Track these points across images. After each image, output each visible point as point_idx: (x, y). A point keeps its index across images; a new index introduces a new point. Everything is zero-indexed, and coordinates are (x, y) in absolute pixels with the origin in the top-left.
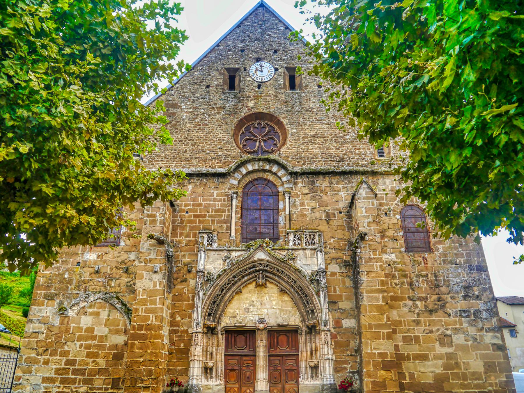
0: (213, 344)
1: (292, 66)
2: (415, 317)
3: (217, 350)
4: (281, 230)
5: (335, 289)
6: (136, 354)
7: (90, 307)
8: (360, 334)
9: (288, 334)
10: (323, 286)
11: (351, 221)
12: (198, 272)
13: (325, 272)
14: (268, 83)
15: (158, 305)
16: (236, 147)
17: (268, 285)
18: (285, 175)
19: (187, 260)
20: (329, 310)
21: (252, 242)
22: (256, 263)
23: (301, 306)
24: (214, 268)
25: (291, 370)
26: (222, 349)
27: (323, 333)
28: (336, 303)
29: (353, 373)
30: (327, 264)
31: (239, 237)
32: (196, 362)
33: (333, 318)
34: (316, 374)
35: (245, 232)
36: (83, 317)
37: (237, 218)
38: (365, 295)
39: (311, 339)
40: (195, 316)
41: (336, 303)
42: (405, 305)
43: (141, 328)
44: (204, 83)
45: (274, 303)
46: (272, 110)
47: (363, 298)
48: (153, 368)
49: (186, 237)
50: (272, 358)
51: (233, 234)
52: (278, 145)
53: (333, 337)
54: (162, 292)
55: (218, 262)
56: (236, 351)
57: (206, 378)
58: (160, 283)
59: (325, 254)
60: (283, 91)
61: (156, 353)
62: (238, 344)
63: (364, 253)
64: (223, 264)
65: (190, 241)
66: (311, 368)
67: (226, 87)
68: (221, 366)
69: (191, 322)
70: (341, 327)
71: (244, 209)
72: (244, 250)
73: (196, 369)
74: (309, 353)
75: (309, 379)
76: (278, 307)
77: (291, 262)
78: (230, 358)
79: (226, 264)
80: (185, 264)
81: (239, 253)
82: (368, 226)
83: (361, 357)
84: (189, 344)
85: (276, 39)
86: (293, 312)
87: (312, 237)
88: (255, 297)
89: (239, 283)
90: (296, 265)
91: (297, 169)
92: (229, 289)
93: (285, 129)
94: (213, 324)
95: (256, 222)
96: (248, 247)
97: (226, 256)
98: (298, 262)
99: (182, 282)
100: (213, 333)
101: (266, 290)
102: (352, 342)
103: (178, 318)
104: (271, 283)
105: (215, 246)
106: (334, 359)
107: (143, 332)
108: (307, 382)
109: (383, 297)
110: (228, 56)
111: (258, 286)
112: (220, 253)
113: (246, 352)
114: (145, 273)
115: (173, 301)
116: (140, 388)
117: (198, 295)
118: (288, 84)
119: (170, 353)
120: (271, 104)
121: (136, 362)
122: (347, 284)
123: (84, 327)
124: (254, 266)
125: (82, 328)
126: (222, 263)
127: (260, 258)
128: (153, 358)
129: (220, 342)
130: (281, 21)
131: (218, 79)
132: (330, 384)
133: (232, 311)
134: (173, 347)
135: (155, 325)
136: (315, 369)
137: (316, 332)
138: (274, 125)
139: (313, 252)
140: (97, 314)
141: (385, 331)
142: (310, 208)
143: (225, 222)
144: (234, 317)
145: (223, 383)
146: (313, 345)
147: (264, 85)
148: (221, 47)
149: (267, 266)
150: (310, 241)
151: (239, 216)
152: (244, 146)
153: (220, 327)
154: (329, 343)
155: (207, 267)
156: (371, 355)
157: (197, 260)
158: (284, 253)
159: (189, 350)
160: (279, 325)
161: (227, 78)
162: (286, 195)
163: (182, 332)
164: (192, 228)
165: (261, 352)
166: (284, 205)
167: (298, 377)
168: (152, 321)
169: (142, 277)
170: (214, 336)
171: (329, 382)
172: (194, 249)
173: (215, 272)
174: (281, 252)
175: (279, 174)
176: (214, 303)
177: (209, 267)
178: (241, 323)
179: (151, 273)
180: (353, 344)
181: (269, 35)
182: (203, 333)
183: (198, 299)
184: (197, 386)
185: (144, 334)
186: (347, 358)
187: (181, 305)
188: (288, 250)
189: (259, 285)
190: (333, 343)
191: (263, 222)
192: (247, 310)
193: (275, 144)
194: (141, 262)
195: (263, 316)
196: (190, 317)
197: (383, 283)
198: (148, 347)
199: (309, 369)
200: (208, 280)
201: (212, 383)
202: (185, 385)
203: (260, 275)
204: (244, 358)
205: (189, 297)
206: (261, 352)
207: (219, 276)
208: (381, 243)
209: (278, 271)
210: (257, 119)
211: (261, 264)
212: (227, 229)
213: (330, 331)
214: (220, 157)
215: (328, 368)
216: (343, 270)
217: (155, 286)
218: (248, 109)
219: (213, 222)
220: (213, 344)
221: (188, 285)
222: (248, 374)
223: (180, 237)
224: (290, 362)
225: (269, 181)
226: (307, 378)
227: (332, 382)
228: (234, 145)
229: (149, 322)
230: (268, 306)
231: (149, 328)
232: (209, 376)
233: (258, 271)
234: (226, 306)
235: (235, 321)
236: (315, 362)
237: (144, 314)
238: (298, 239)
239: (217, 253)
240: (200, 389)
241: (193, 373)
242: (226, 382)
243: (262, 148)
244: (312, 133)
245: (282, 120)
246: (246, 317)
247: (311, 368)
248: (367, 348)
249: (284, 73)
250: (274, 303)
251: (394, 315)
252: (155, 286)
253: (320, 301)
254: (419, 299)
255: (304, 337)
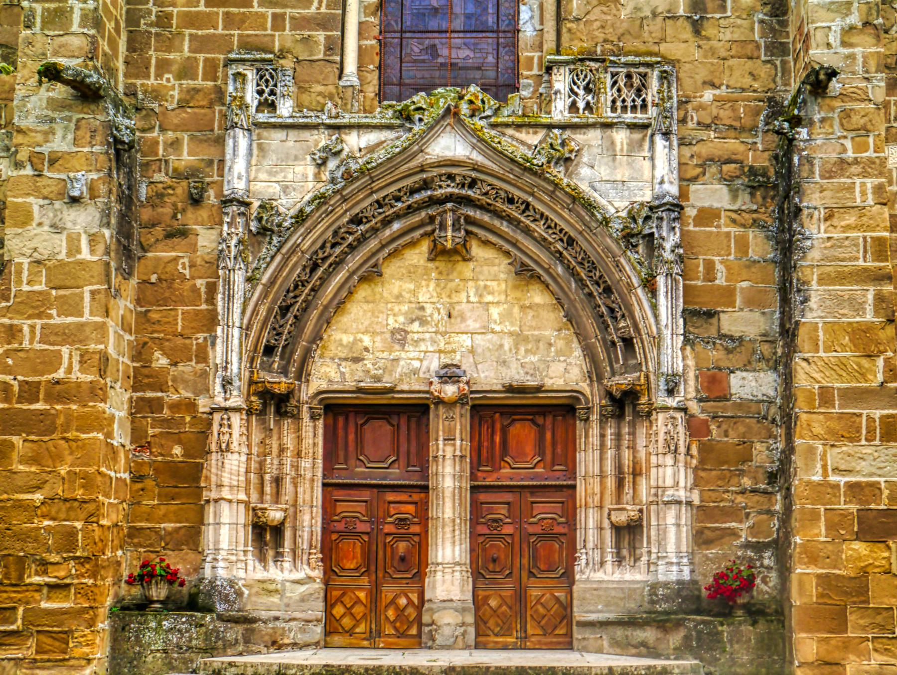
0: (282, 450)
3: (296, 468)
4: (524, 54)
5: (710, 267)
6: (19, 481)
8: (788, 420)
9: (540, 421)
10: (668, 255)
11: (784, 24)
12: (227, 202)
13: (677, 207)
15: (87, 317)
17: (476, 250)
19: (186, 158)
20: (687, 341)
21: (420, 99)
22: (435, 172)
23: (590, 325)
24: (285, 189)
25: (548, 536)
26: (312, 467)
27: (661, 418)
28: (710, 315)
29: (759, 548)
30: (685, 181)
31: (373, 78)
32: (225, 506)
33: (698, 368)
34: (633, 548)
35: (393, 61)
38: (816, 292)
39: (618, 436)
40: (217, 354)
41: (710, 315)
43: (30, 392)
45: (495, 312)
47: (806, 300)
48: (79, 525)
49: (180, 76)
50: (483, 497)
51: (351, 66)
53: (695, 428)
54: (99, 270)
55: (299, 169)
56: (361, 472)
57: (262, 558)
58: (93, 240)
59: (682, 143)
61: (85, 476)
62: (369, 449)
63: (822, 142)
64: (317, 177)
65: (197, 91)
66: (617, 529)
68: (310, 522)
69: (204, 374)
70: (725, 397)
72: (389, 127)
73: (225, 531)
74: (611, 483)
75: (609, 566)
76: (508, 327)
77: (557, 172)
78: (339, 494)
79: (326, 176)
80: (178, 175)
81: (373, 137)
82: (844, 44)
83: (788, 496)
84: (199, 445)
86: (561, 344)
87: (636, 81)
88: (427, 293)
89: (373, 244)
90: (574, 181)
92: (339, 263)
94: (281, 383)
95: (433, 24)
96: (405, 117)
97: (325, 149)
98: (585, 171)
99: (169, 236)
100: (281, 414)
101: (467, 269)
102: (758, 446)
103: (161, 361)
104: (486, 243)
105: (285, 108)
106: (697, 502)
107: (39, 406)
108: (599, 575)
109: (880, 298)
111: (438, 253)
112: (305, 134)
113: (395, 475)
114: (35, 203)
115: (139, 302)
116: (39, 588)
117: (228, 282)
119: (137, 478)
121: (20, 505)
122: (754, 253)
124: (426, 185)
126: (311, 170)
127: (449, 154)
128: (79, 493)
129: (308, 441)
132: (679, 582)
133: (346, 339)
134: (146, 457)
135: (79, 385)
136: (629, 535)
137: (637, 414)
139: (637, 136)
141: (877, 414)
143: (323, 23)
144: (357, 360)
145: (318, 574)
146: (626, 454)
149: (473, 184)
150: (629, 95)
153: (306, 392)
154: (682, 449)
155: (257, 187)
156: (825, 490)
157: (222, 161)
158: (534, 138)
159: (199, 468)
160: (510, 389)
163: (175, 407)
164: (200, 44)
165: (449, 476)
167: (572, 559)
168: (69, 370)
169: (25, 218)
170: (287, 423)
171: (673, 577)
172: (213, 120)
173: (288, 205)
174: (522, 135)
176: (285, 310)
177: (265, 187)
178: (378, 379)
179: (58, 205)
180: (763, 454)
182: (249, 412)
183: (230, 298)
184: (232, 583)
185: (42, 413)
186: (739, 498)
187: (167, 316)
188: (550, 127)
189: (445, 252)
190: (694, 451)
191: (458, 24)
192: (400, 337)
194: (18, 165)
195: (457, 358)
196: (202, 356)
197: (880, 248)
198: (57, 458)
199: (608, 534)
200: (264, 231)
201: (282, 573)
202: (192, 579)
204: (390, 497)
205: (195, 290)
206: (449, 476)
207: (301, 218)
208: (886, 105)
209: (511, 201)
211: (451, 177)
212: (329, 49)
213: (685, 410)
215: (672, 531)
216: (744, 201)
217: (74, 249)
219: (278, 19)
220: (282, 450)
221: (194, 248)
222: (402, 547)
223: (159, 76)
224: (545, 511)
226: (602, 563)
227: (686, 575)
229: (60, 374)
230: (472, 325)
231: (60, 392)
232: (271, 553)
233: (441, 201)
234: (326, 321)
235: (360, 374)
236: (631, 511)
237: (38, 346)
238: (587, 90)
239: (293, 134)
240: (239, 594)
241: (217, 542)
242: (329, 574)
246: (396, 360)
247: (617, 529)
248: (809, 468)
250: (495, 312)
252: (74, 249)
253: (654, 307)
255: (595, 430)
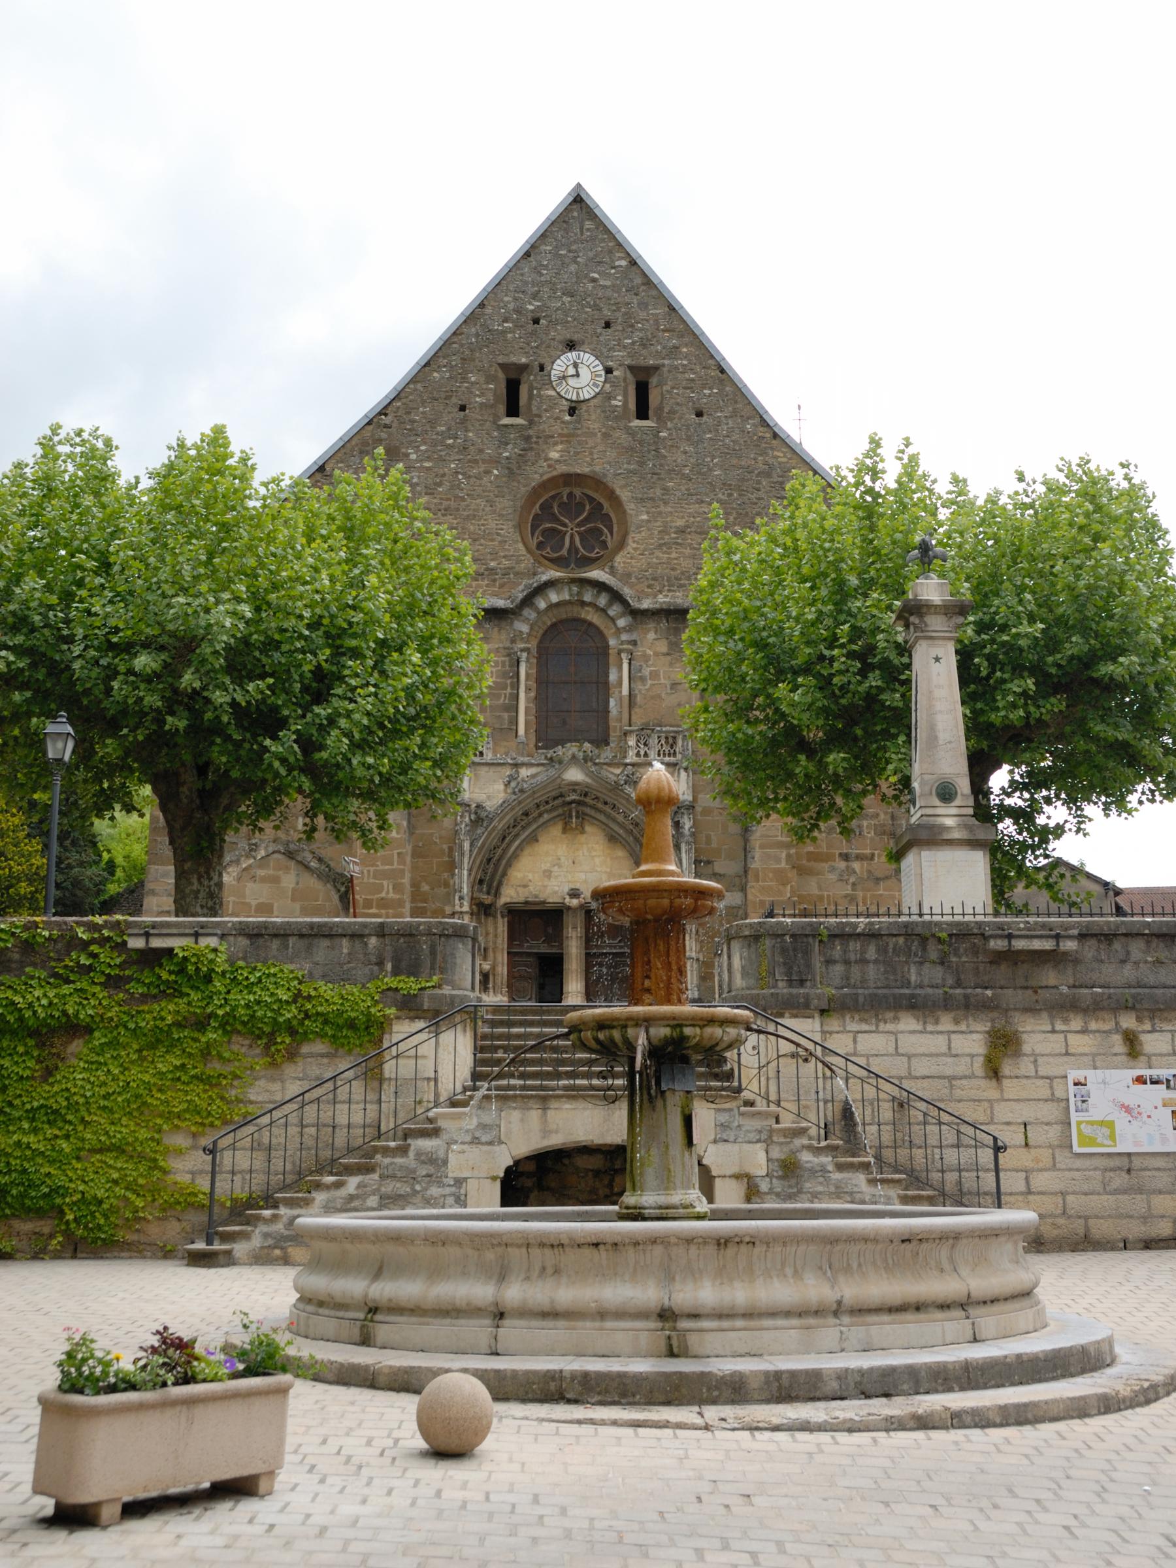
0: (487, 934)
1: (641, 362)
2: (848, 890)
4: (612, 724)
5: (708, 838)
7: (260, 867)
14: (592, 403)
15: (395, 866)
16: (523, 551)
17: (588, 828)
18: (623, 615)
24: (489, 797)
26: (502, 941)
28: (708, 862)
36: (250, 885)
37: (527, 699)
38: (758, 854)
41: (708, 862)
42: (833, 869)
44: (454, 400)
46: (597, 468)
52: (609, 544)
59: (694, 773)
60: (622, 424)
67: (502, 409)
68: (503, 970)
71: (542, 683)
81: (533, 770)
85: (609, 293)
89: (534, 826)
91: (646, 604)
92: (517, 836)
93: (624, 512)
94: (487, 899)
97: (510, 776)
100: (487, 914)
101: (583, 838)
103: (425, 888)
109: (789, 856)
110: (504, 332)
117: (461, 846)
118: (632, 406)
120: (598, 458)
123: (254, 903)
124: (561, 795)
125: (249, 905)
126: (502, 787)
129: (500, 929)
130: (619, 245)
131: (485, 392)
133: (520, 875)
138: (602, 501)
140: (276, 880)
142: (668, 683)
144: (525, 886)
147: (584, 407)
148: (488, 310)
150: (666, 748)
151: (533, 694)
152: (540, 546)
158: (618, 771)
161: (503, 385)
162: (624, 656)
166: (620, 676)
170: (490, 919)
175: (611, 613)
176: (489, 860)
181: (594, 280)
183: (462, 854)
188: (627, 765)
193: (604, 542)
203: (571, 809)
210: (566, 484)
212: (510, 722)
214: (492, 570)
218: (549, 466)
225: (590, 624)
228: (521, 546)
229: (383, 895)
234: (509, 865)
239: (493, 769)
243: (577, 551)
244: (680, 523)
245: (618, 491)
249: (625, 380)
250: (597, 860)
251: (812, 887)
254: (859, 857)
